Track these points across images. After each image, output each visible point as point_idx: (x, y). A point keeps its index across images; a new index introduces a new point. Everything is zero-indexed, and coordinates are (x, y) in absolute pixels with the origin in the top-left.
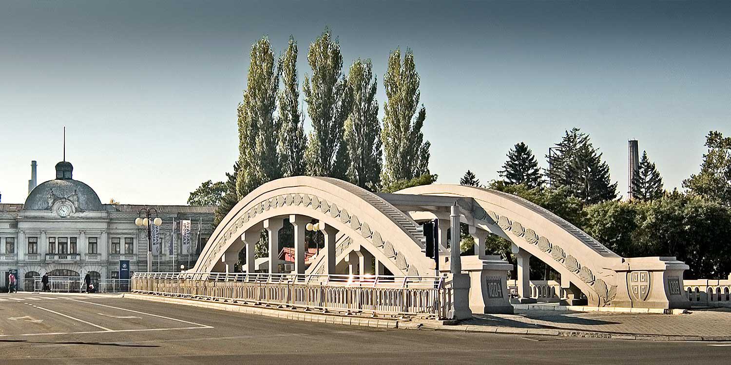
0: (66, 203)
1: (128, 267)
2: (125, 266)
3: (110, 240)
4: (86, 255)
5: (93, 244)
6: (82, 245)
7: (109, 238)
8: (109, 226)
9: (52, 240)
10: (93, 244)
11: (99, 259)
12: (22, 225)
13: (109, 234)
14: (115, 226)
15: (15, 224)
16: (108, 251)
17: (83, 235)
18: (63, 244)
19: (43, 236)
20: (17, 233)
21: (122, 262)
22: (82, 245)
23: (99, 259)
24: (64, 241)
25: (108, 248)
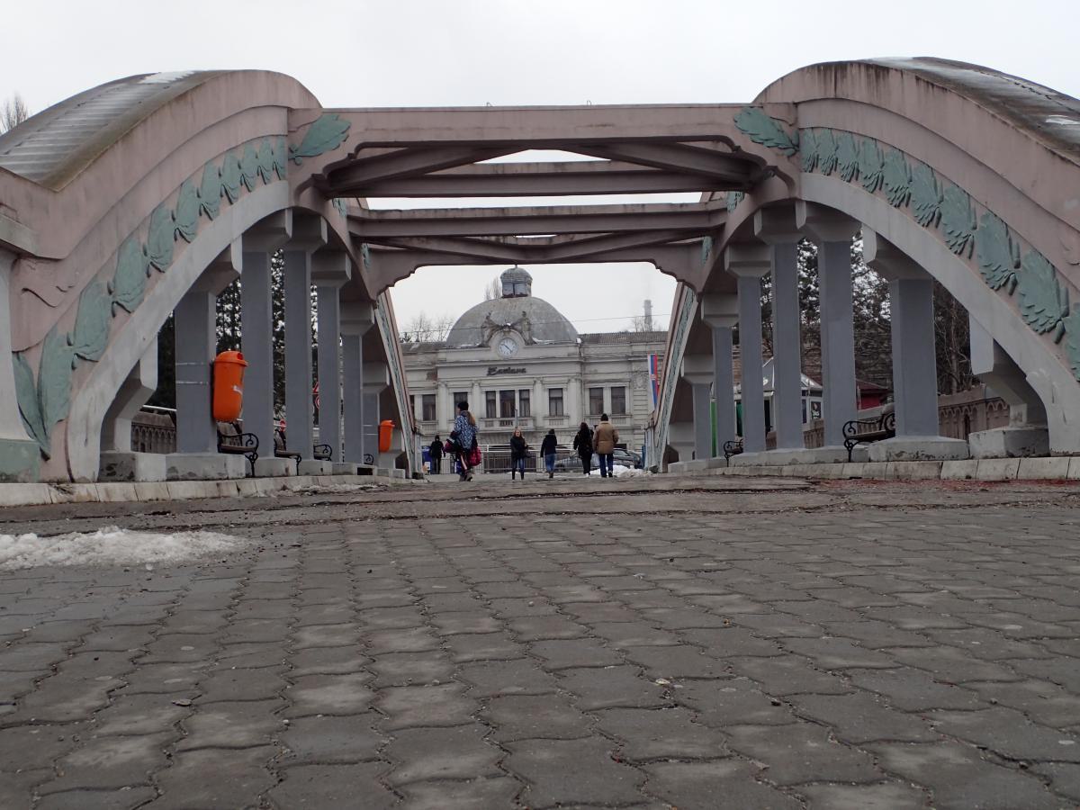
0: (511, 333)
3: (587, 394)
4: (545, 418)
5: (556, 398)
6: (540, 403)
9: (491, 397)
10: (556, 398)
12: (441, 374)
13: (583, 383)
14: (592, 368)
15: (433, 375)
16: (583, 410)
17: (538, 386)
19: (476, 389)
20: (437, 388)
22: (540, 403)
25: (583, 404)
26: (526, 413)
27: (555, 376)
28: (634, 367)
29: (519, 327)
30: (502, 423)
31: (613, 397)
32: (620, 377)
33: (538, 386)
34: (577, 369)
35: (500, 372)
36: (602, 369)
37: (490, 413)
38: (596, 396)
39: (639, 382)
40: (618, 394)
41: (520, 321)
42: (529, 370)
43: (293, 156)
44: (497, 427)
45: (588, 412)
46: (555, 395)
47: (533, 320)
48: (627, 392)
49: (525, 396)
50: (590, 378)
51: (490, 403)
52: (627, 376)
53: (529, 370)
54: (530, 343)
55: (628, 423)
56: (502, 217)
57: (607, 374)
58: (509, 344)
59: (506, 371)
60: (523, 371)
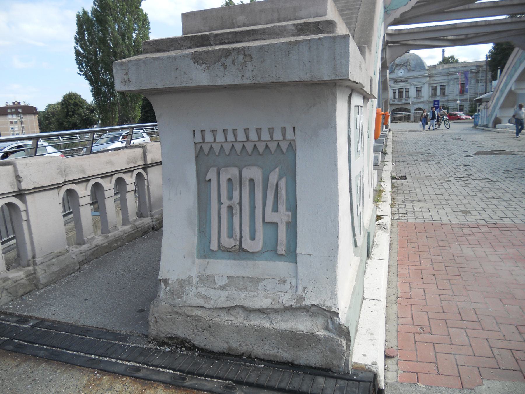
1: (438, 104)
2: (436, 103)
3: (431, 88)
4: (414, 98)
5: (419, 91)
6: (413, 92)
7: (429, 86)
8: (430, 79)
9: (394, 91)
10: (419, 91)
11: (422, 100)
13: (430, 84)
14: (433, 78)
17: (412, 87)
18: (401, 93)
21: (435, 101)
22: (413, 92)
23: (422, 100)
24: (402, 90)
26: (408, 97)
27: (418, 83)
28: (450, 77)
29: (406, 64)
30: (398, 101)
31: (441, 89)
32: (444, 81)
33: (412, 87)
34: (428, 79)
35: (398, 82)
36: (437, 78)
37: (394, 97)
38: (435, 89)
39: (451, 83)
40: (443, 89)
41: (407, 62)
42: (409, 80)
43: (386, 10)
44: (396, 102)
45: (431, 95)
46: (419, 89)
47: (411, 62)
48: (446, 87)
49: (407, 90)
50: (432, 82)
51: (394, 93)
52: (447, 81)
53: (409, 80)
54: (409, 70)
55: (446, 98)
56: (454, 27)
57: (438, 80)
58: (402, 71)
59: (400, 81)
60: (407, 81)
